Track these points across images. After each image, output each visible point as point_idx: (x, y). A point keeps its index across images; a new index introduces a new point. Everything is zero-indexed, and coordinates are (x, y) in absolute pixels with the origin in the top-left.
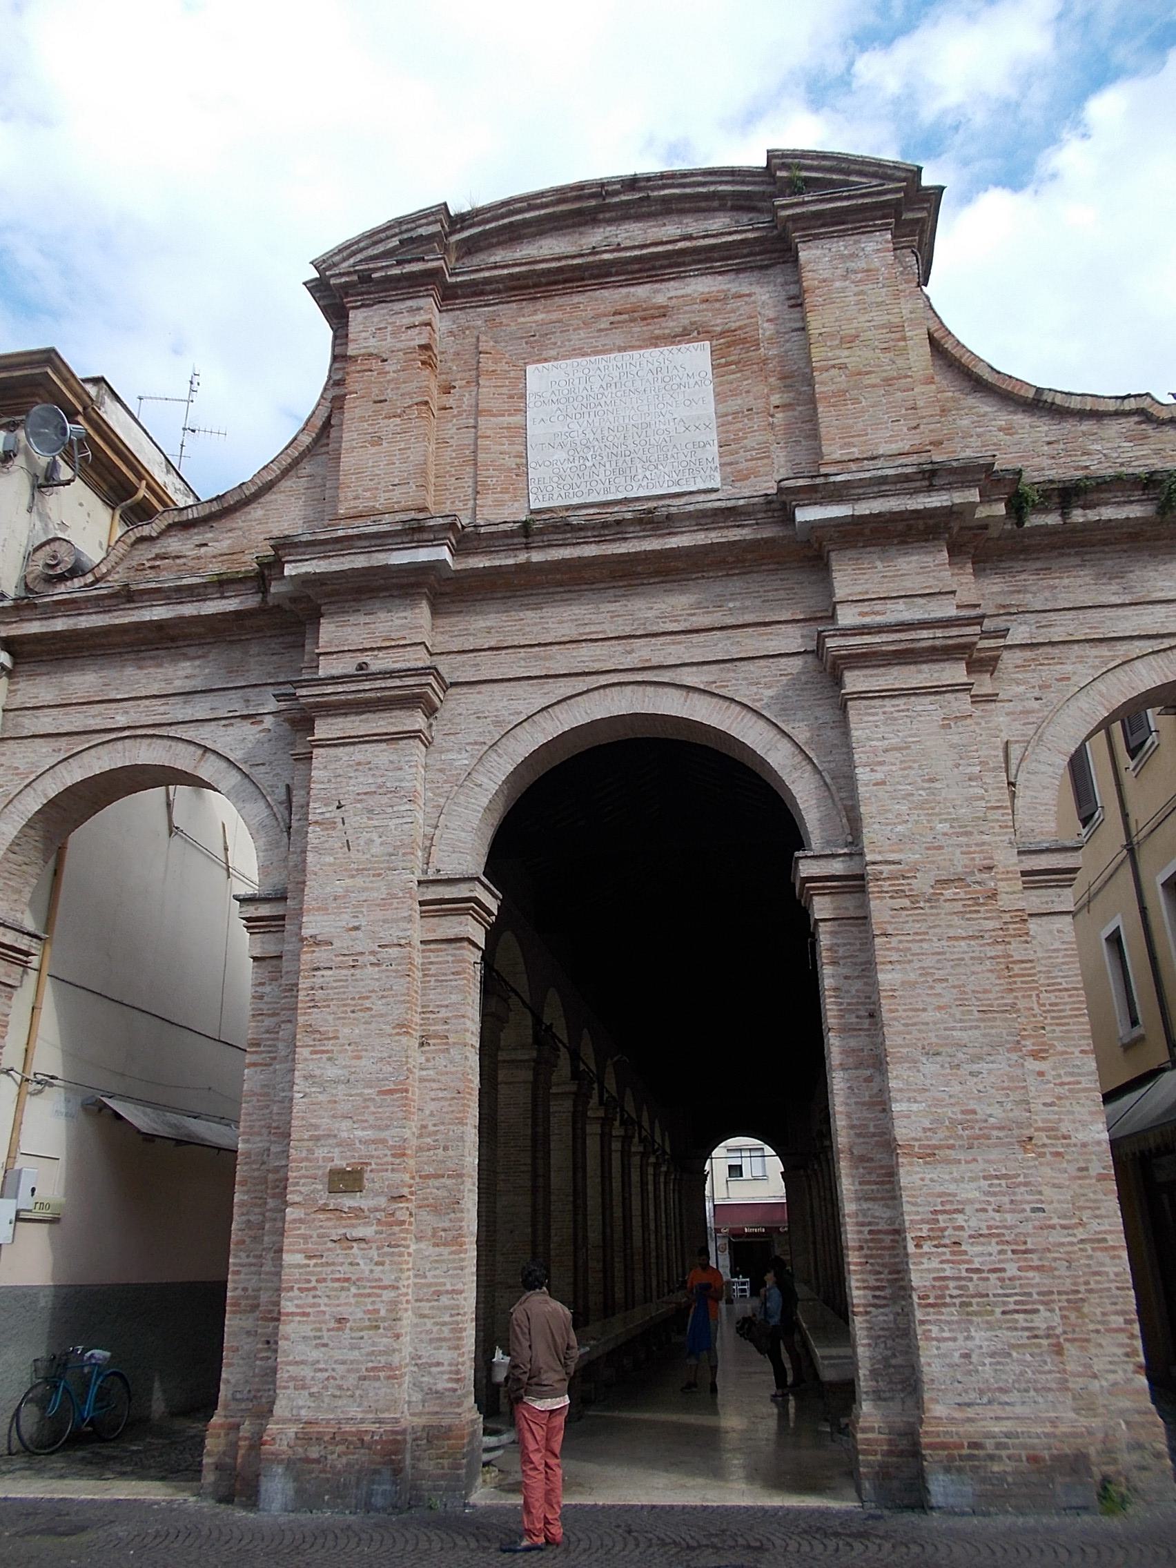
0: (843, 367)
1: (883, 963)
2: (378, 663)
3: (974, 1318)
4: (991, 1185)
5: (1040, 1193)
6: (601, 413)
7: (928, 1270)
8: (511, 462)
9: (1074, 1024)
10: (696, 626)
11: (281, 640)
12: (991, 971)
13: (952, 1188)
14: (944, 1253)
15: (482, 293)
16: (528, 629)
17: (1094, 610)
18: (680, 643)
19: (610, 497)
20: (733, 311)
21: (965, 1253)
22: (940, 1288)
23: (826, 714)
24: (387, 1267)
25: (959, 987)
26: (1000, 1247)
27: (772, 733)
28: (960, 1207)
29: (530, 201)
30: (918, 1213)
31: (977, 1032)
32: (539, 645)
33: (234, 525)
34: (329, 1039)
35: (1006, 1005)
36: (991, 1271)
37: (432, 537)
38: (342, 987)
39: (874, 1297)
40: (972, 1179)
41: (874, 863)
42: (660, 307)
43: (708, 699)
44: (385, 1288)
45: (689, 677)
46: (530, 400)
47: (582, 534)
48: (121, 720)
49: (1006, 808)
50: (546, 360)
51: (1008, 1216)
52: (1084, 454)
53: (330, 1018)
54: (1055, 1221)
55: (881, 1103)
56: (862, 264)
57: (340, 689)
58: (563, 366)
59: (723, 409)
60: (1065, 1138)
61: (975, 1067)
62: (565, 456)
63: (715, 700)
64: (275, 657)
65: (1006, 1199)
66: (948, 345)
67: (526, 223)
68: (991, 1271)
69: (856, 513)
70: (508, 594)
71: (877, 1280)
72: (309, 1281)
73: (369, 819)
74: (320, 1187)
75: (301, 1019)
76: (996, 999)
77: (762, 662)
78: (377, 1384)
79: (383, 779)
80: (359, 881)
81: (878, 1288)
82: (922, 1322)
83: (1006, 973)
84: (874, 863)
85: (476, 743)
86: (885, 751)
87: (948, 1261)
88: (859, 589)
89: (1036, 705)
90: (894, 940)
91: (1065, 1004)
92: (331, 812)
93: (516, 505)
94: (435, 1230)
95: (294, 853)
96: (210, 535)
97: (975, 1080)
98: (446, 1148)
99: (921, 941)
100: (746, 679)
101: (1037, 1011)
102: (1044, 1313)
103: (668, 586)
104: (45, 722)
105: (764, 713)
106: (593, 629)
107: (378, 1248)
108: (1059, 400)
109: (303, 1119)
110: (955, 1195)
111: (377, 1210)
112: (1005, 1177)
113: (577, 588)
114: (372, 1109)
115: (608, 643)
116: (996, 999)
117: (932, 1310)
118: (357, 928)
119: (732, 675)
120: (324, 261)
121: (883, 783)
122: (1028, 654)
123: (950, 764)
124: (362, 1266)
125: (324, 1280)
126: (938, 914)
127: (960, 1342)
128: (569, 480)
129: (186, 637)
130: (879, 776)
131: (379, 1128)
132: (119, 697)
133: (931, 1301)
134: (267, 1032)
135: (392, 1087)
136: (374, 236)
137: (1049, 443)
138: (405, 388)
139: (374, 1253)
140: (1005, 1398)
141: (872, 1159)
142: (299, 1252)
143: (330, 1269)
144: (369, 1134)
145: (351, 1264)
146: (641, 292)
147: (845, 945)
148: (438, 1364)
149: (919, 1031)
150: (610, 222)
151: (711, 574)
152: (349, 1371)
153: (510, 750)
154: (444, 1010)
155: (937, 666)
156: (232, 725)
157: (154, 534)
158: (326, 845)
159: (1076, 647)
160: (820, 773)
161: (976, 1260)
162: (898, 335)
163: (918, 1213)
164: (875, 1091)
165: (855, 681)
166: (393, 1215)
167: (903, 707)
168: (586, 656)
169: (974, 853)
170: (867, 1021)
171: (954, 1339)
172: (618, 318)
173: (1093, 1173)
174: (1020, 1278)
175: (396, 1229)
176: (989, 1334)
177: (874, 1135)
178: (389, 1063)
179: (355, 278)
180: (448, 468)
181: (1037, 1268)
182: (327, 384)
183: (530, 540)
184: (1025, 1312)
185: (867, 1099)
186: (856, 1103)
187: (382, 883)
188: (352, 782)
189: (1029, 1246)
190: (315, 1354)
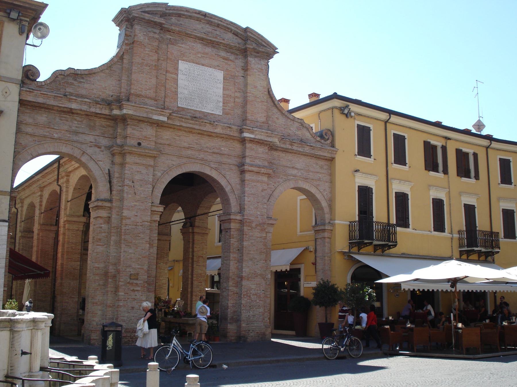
6: (197, 83)
7: (245, 301)
11: (105, 123)
13: (251, 286)
21: (251, 298)
24: (143, 296)
36: (255, 301)
38: (133, 230)
40: (254, 284)
46: (179, 72)
50: (184, 60)
51: (259, 291)
52: (290, 130)
55: (240, 269)
61: (257, 263)
64: (104, 128)
67: (184, 15)
68: (255, 301)
72: (125, 299)
73: (141, 187)
74: (128, 278)
75: (123, 237)
80: (137, 204)
81: (233, 304)
82: (243, 310)
84: (246, 219)
89: (273, 187)
90: (248, 236)
100: (223, 168)
103: (209, 139)
112: (259, 284)
114: (140, 261)
121: (250, 201)
127: (248, 313)
128: (188, 101)
130: (249, 200)
132: (55, 128)
134: (103, 237)
135: (145, 256)
137: (284, 125)
139: (140, 293)
141: (235, 279)
143: (130, 296)
144: (139, 267)
145: (135, 295)
157: (65, 75)
164: (237, 266)
170: (237, 251)
171: (247, 313)
190: (127, 315)
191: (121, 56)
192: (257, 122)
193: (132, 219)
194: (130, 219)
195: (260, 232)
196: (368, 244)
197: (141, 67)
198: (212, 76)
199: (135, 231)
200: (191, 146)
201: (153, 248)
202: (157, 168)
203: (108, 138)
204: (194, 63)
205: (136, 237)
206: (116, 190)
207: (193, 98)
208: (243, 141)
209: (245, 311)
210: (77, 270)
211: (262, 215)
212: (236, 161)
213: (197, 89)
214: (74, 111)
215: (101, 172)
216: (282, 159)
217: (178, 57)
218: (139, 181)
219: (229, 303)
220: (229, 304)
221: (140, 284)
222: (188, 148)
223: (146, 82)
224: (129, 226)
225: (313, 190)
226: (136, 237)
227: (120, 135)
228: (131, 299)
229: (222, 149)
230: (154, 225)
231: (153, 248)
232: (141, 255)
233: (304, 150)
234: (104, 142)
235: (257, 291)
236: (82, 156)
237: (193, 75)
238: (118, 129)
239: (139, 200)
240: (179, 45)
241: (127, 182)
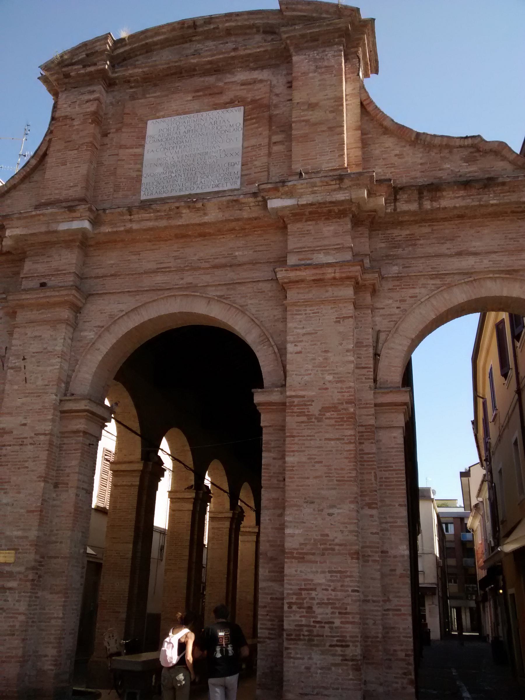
1: (289, 451)
3: (314, 648)
4: (331, 576)
8: (134, 174)
9: (397, 489)
13: (310, 576)
14: (303, 612)
22: (298, 630)
24: (22, 603)
25: (328, 466)
26: (332, 610)
28: (314, 587)
29: (156, 31)
30: (291, 589)
34: (6, 482)
35: (351, 477)
36: (326, 623)
39: (269, 634)
40: (323, 572)
44: (20, 614)
46: (148, 140)
50: (158, 118)
51: (339, 593)
55: (281, 528)
56: (326, 63)
59: (246, 145)
61: (331, 511)
62: (162, 171)
64: (8, 279)
65: (339, 584)
67: (155, 44)
68: (326, 623)
71: (272, 625)
73: (38, 366)
76: (347, 473)
80: (29, 399)
84: (291, 397)
86: (304, 335)
87: (304, 616)
89: (397, 311)
90: (296, 439)
91: (393, 478)
92: (19, 363)
93: (134, 198)
97: (330, 518)
99: (311, 440)
110: (312, 580)
116: (347, 473)
117: (293, 642)
119: (233, 292)
126: (321, 425)
127: (306, 660)
130: (299, 349)
133: (292, 637)
139: (16, 596)
140: (326, 692)
144: (20, 533)
147: (275, 440)
161: (319, 616)
167: (316, 311)
169: (345, 392)
171: (303, 659)
174: (341, 628)
176: (323, 657)
181: (352, 623)
183: (132, 217)
184: (342, 646)
185: (278, 526)
189: (348, 611)
193: (15, 432)
194: (12, 432)
195: (333, 425)
198: (218, 123)
201: (67, 491)
202: (87, 324)
205: (19, 468)
210: (127, 559)
211: (341, 382)
218: (36, 354)
221: (19, 573)
222: (155, 272)
224: (9, 448)
226: (19, 468)
229: (237, 254)
230: (74, 442)
231: (67, 491)
235: (333, 593)
239: (32, 393)
241: (13, 362)
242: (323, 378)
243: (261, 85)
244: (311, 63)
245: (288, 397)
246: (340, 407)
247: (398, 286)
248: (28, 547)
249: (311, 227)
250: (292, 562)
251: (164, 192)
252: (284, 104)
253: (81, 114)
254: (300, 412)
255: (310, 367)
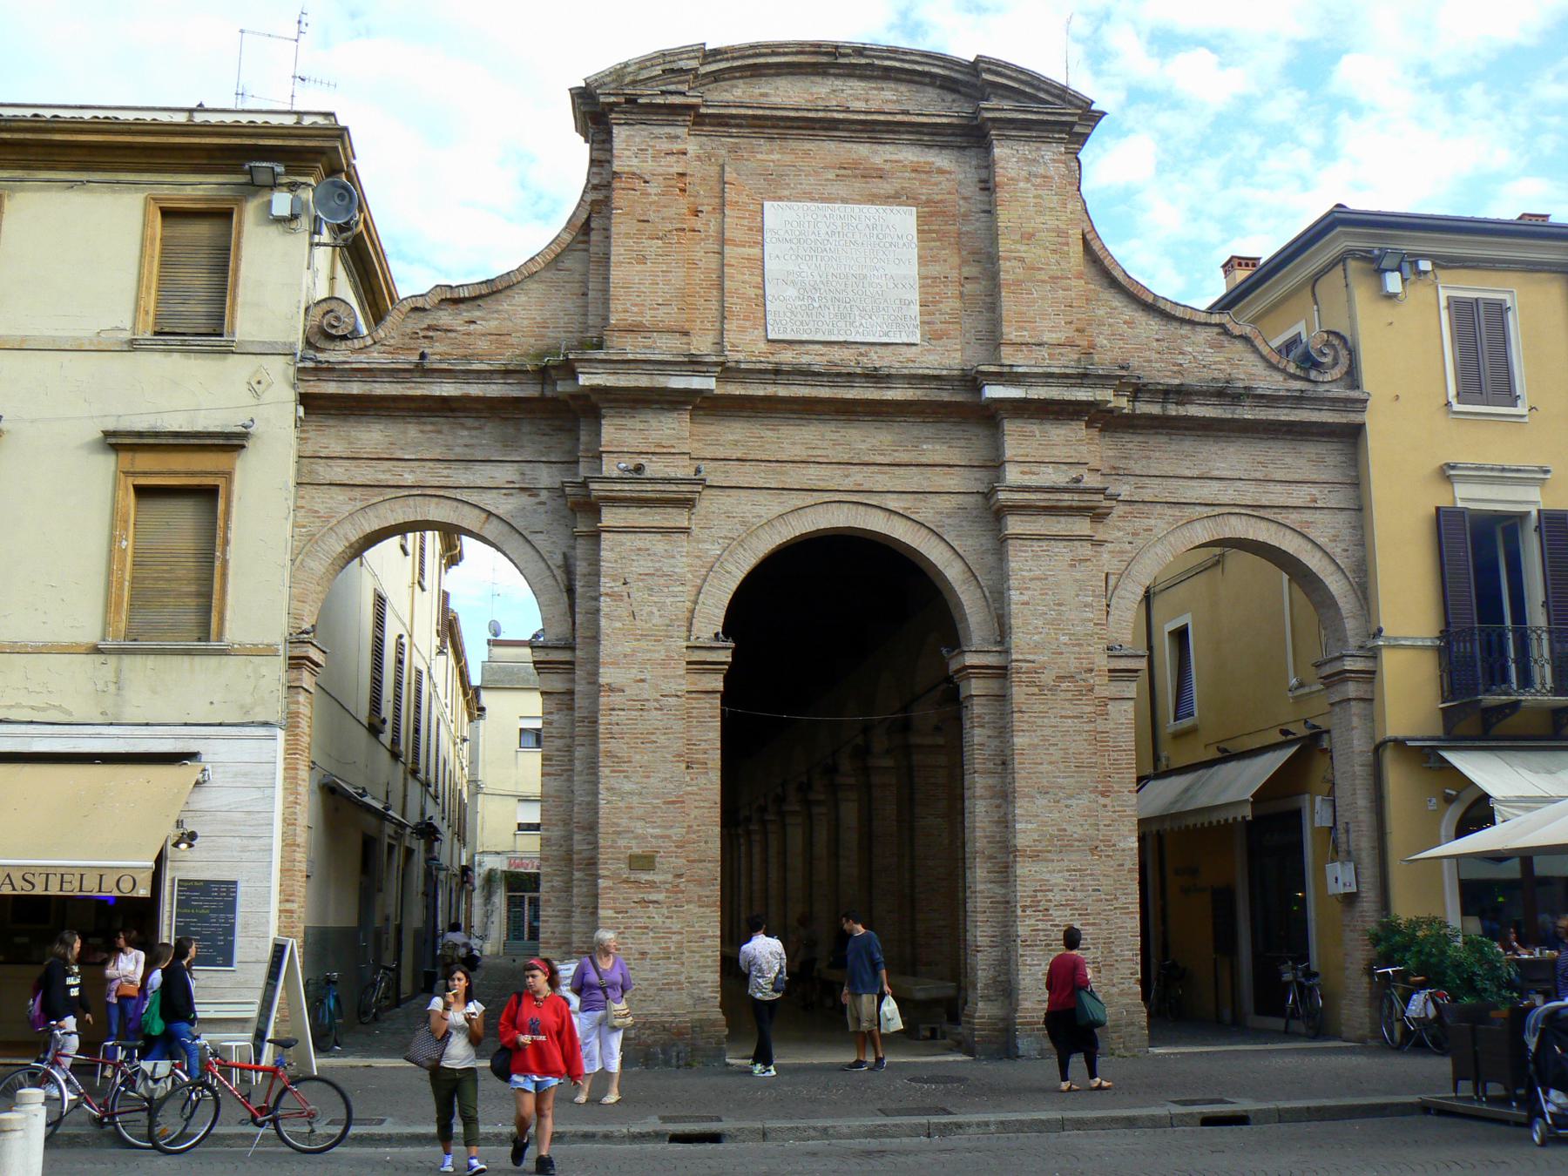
0: (1022, 260)
1: (1018, 731)
2: (654, 468)
5: (1099, 880)
6: (826, 259)
7: (1029, 926)
8: (752, 292)
10: (897, 461)
11: (550, 422)
12: (1086, 740)
13: (1047, 876)
15: (727, 125)
16: (767, 446)
17: (1173, 479)
18: (885, 473)
19: (833, 338)
20: (936, 184)
21: (1051, 915)
22: (1034, 935)
23: (987, 542)
24: (674, 920)
27: (948, 554)
29: (775, 49)
30: (1025, 891)
31: (1072, 780)
32: (777, 461)
33: (500, 308)
37: (705, 369)
40: (1059, 872)
41: (1017, 661)
42: (880, 169)
43: (904, 521)
44: (674, 933)
45: (893, 503)
46: (767, 236)
47: (820, 378)
48: (409, 479)
49: (1103, 625)
50: (780, 199)
51: (1078, 894)
52: (1180, 353)
53: (625, 746)
54: (1103, 896)
55: (1006, 823)
56: (1041, 170)
57: (626, 487)
58: (795, 208)
60: (1114, 845)
61: (1069, 802)
63: (909, 523)
64: (545, 438)
65: (1079, 883)
66: (1096, 246)
67: (767, 65)
69: (1029, 397)
70: (753, 414)
75: (602, 746)
77: (946, 497)
78: (671, 993)
79: (660, 564)
80: (643, 644)
81: (993, 937)
82: (1022, 956)
83: (1094, 742)
84: (1017, 661)
85: (726, 538)
86: (1031, 580)
88: (1021, 452)
89: (1128, 547)
90: (1026, 715)
92: (618, 587)
94: (700, 897)
95: (579, 613)
96: (478, 313)
98: (706, 842)
100: (933, 508)
101: (1107, 766)
102: (1092, 950)
104: (338, 472)
105: (945, 537)
106: (819, 452)
107: (668, 908)
108: (1168, 308)
109: (607, 818)
110: (1048, 881)
111: (666, 883)
112: (1080, 870)
113: (807, 416)
114: (660, 814)
115: (830, 466)
118: (642, 681)
120: (596, 80)
121: (1027, 603)
122: (1127, 508)
123: (1073, 593)
124: (657, 919)
125: (630, 928)
129: (464, 410)
130: (1025, 598)
131: (665, 827)
132: (406, 457)
136: (644, 63)
137: (1158, 340)
138: (667, 212)
139: (665, 911)
142: (610, 908)
144: (658, 831)
145: (649, 917)
146: (862, 150)
148: (704, 982)
149: (1037, 778)
150: (836, 76)
151: (912, 419)
152: (650, 985)
153: (753, 546)
154: (703, 743)
155: (1070, 519)
156: (511, 495)
157: (428, 307)
158: (616, 613)
159: (1158, 506)
160: (981, 588)
162: (1063, 240)
163: (1025, 891)
165: (1014, 525)
166: (677, 886)
168: (812, 475)
171: (1040, 965)
172: (842, 172)
173: (1126, 867)
175: (680, 895)
177: (999, 842)
178: (671, 782)
179: (622, 100)
180: (698, 289)
182: (586, 187)
186: (990, 821)
187: (662, 648)
188: (635, 564)
191: (583, 224)
192: (1039, 345)
196: (1507, 711)
197: (637, 243)
198: (879, 228)
199: (640, 726)
200: (815, 452)
201: (707, 773)
203: (560, 465)
204: (813, 200)
206: (583, 611)
207: (816, 305)
208: (990, 417)
209: (1029, 959)
211: (1080, 645)
212: (976, 479)
213: (830, 277)
214: (454, 405)
215: (542, 565)
216: (1158, 454)
217: (761, 194)
219: (978, 933)
220: (979, 939)
221: (666, 883)
223: (653, 284)
225: (1289, 544)
227: (587, 450)
228: (636, 928)
229: (925, 447)
231: (707, 773)
232: (658, 798)
233: (1233, 413)
234: (546, 477)
236: (484, 523)
237: (813, 237)
238: (582, 433)
240: (759, 156)
242: (1057, 639)
243: (941, 178)
244: (1020, 164)
245: (1012, 661)
246: (1079, 677)
247: (1131, 513)
248: (675, 849)
249: (1035, 428)
250: (1024, 862)
251: (805, 331)
252: (977, 216)
253: (661, 175)
254: (1030, 682)
255: (1040, 623)
